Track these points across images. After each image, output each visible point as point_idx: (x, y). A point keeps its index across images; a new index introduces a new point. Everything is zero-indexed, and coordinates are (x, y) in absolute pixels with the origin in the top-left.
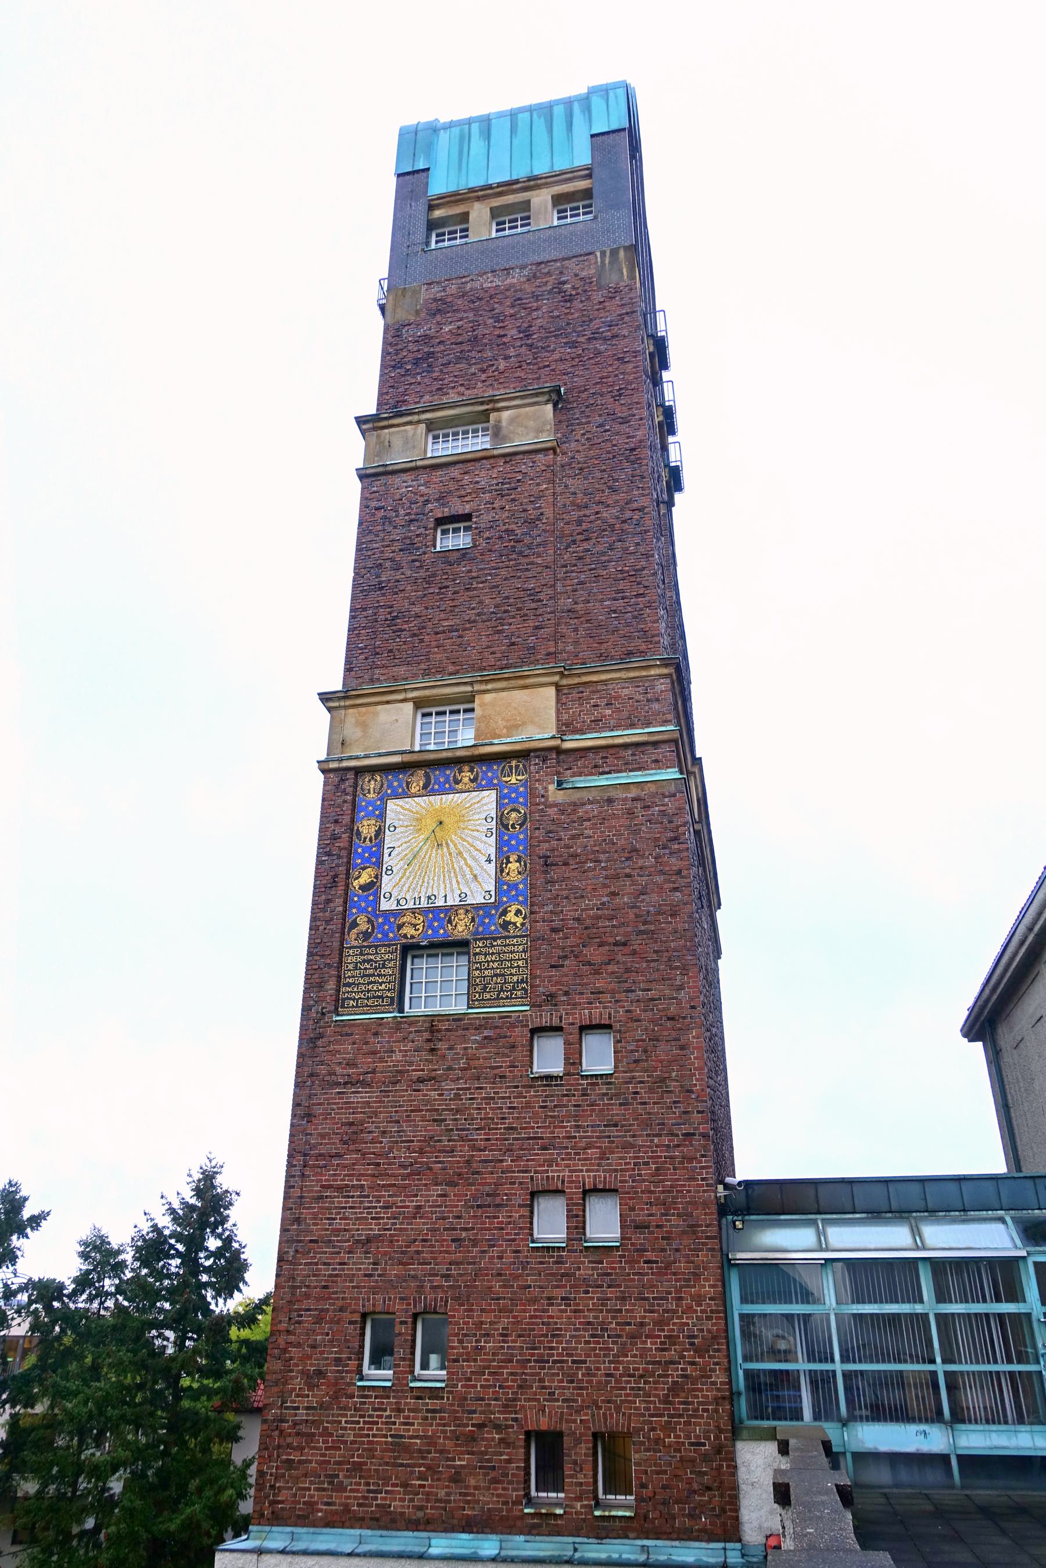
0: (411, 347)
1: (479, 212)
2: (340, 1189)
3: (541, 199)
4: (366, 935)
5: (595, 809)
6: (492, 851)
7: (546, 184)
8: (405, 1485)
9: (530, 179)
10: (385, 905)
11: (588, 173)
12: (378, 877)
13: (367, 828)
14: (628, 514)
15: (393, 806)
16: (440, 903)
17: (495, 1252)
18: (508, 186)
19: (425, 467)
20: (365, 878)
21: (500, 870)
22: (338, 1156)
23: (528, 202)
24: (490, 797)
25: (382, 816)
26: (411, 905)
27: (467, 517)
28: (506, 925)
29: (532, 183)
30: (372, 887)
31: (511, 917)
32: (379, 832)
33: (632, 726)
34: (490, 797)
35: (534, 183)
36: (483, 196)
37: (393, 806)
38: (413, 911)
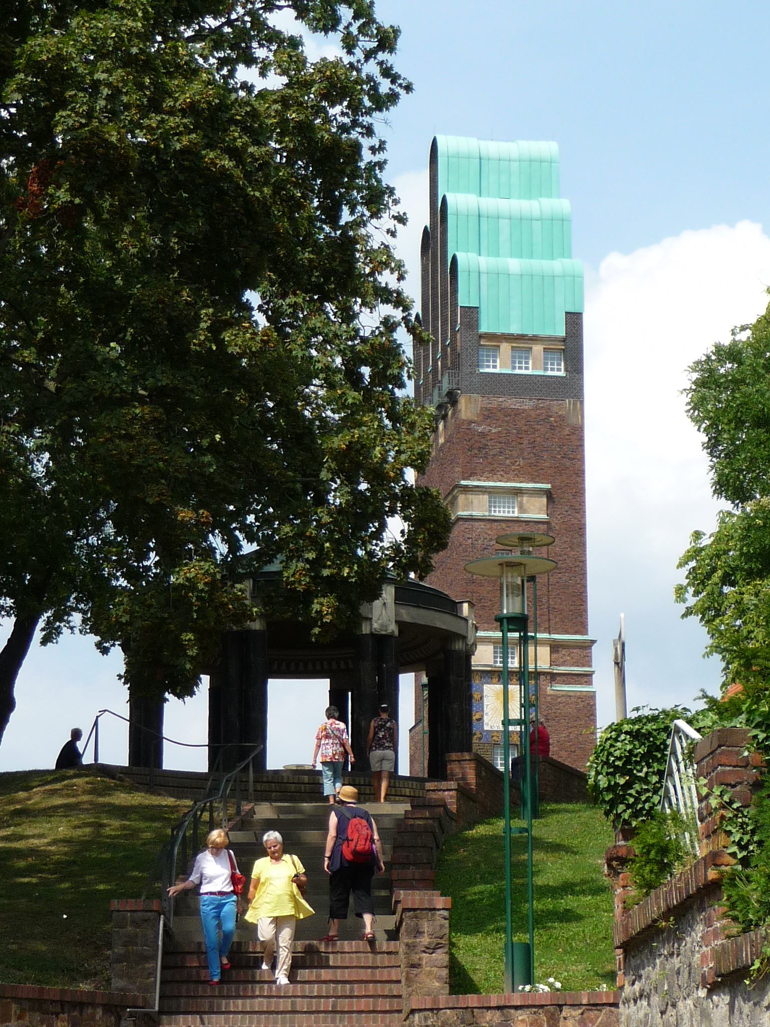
0: (477, 438)
1: (505, 347)
3: (538, 349)
4: (480, 739)
5: (564, 699)
9: (534, 336)
10: (486, 728)
11: (564, 340)
14: (578, 563)
15: (486, 687)
18: (521, 338)
19: (489, 520)
23: (531, 348)
30: (480, 719)
32: (482, 698)
33: (578, 666)
35: (535, 339)
37: (486, 687)
38: (497, 731)
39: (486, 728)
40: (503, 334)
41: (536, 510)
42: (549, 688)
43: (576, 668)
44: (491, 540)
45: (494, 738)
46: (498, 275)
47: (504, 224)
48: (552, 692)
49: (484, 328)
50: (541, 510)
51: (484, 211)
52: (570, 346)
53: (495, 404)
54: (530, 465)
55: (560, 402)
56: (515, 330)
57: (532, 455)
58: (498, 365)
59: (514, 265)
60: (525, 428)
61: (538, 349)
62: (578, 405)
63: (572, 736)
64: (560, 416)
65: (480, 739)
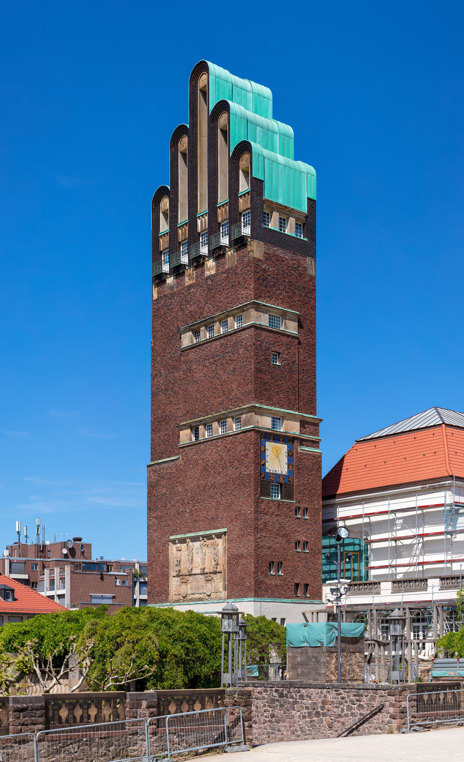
2: (265, 537)
4: (264, 478)
6: (287, 461)
8: (278, 591)
10: (267, 471)
12: (265, 462)
13: (262, 449)
16: (277, 473)
17: (290, 552)
20: (262, 463)
21: (288, 467)
22: (263, 530)
24: (286, 446)
25: (265, 446)
26: (272, 472)
27: (279, 353)
28: (289, 481)
30: (264, 465)
31: (290, 479)
32: (265, 450)
34: (286, 446)
38: (272, 474)
39: (267, 471)
41: (291, 328)
42: (299, 448)
43: (311, 437)
44: (270, 344)
45: (271, 478)
48: (300, 451)
50: (295, 329)
52: (308, 223)
54: (290, 297)
55: (304, 258)
57: (289, 291)
60: (286, 271)
61: (292, 221)
62: (313, 263)
63: (310, 481)
64: (304, 267)
65: (264, 478)
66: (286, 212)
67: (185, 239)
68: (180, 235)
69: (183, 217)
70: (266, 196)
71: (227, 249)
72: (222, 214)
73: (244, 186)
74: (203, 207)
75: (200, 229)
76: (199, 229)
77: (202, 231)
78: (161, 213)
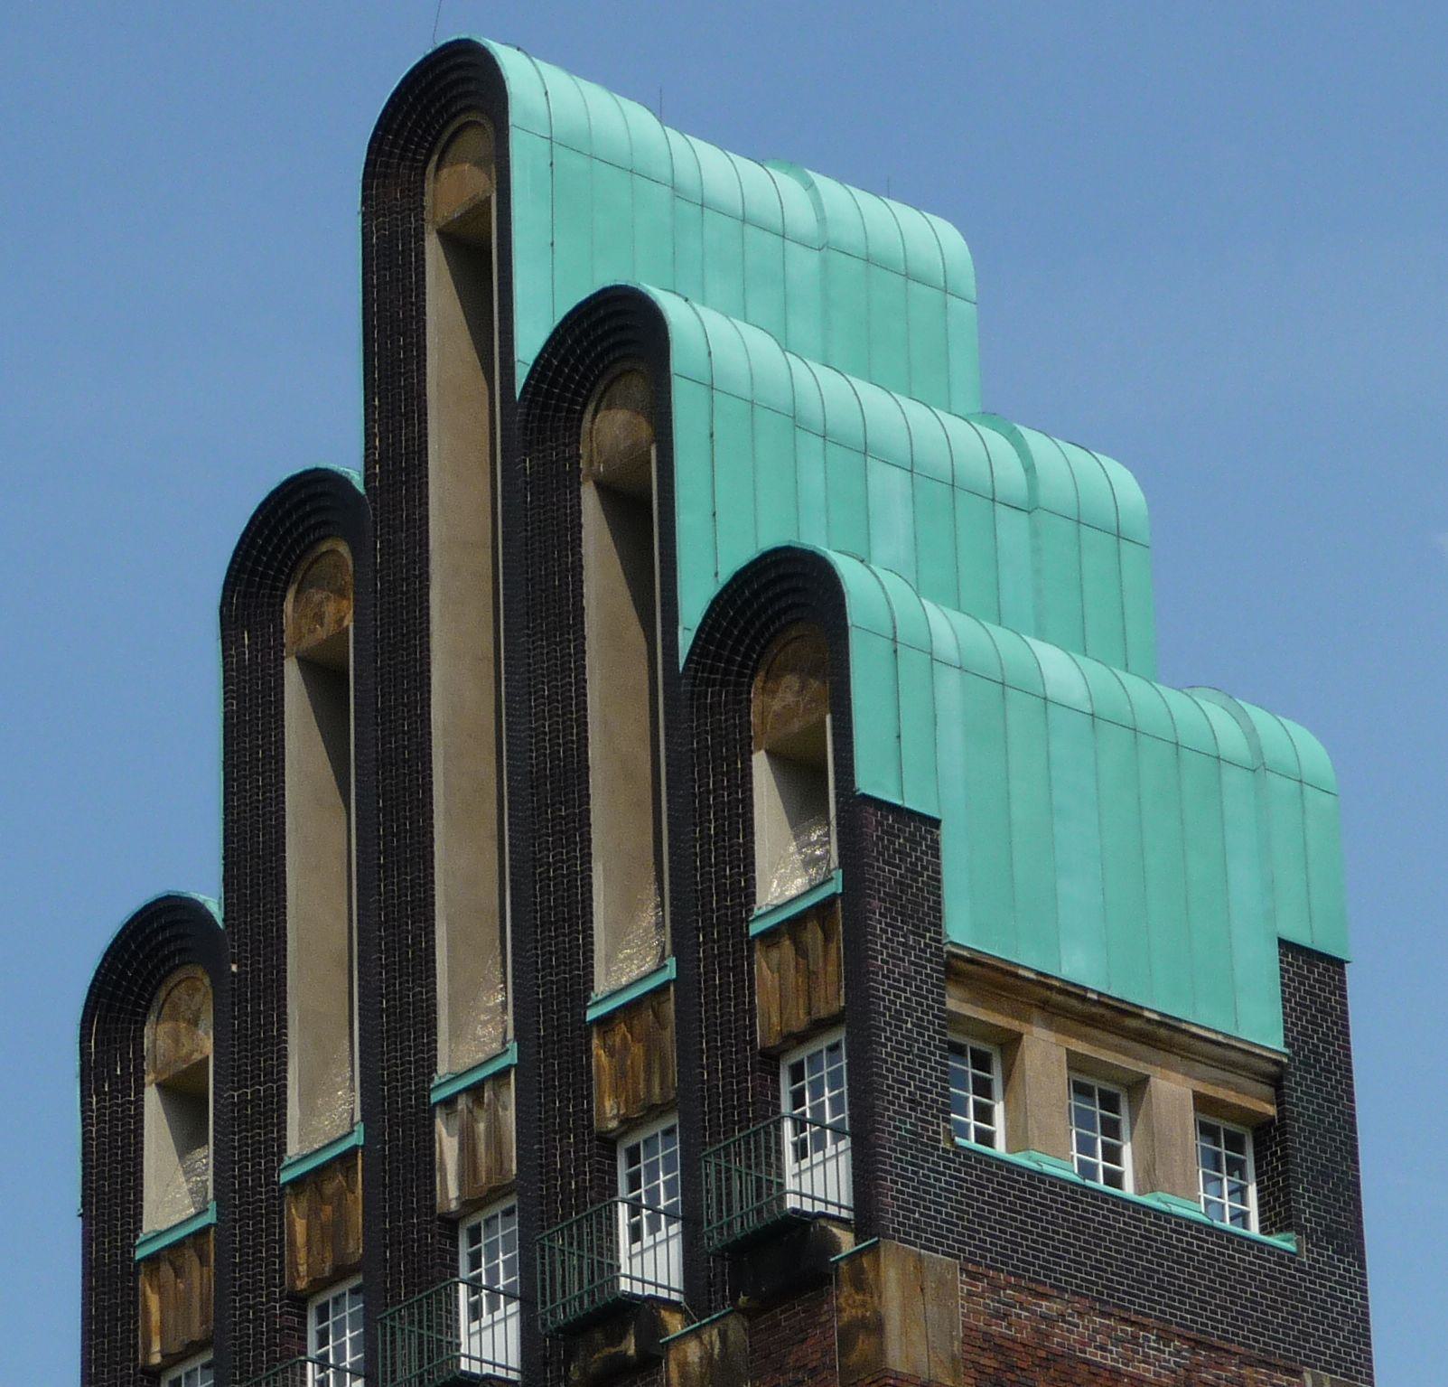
1: (1044, 1052)
7: (1186, 1049)
9: (1169, 1024)
11: (1276, 1078)
23: (1138, 1086)
29: (1163, 1032)
35: (1166, 1038)
36: (1057, 1006)
40: (1043, 980)
46: (1002, 685)
47: (888, 483)
49: (963, 926)
51: (810, 408)
52: (1292, 1122)
53: (1019, 1328)
56: (1079, 965)
58: (1029, 1127)
59: (1058, 668)
61: (1172, 1091)
66: (1117, 1040)
67: (341, 1273)
68: (300, 1239)
69: (322, 1112)
70: (963, 926)
71: (675, 1324)
72: (621, 1074)
73: (786, 870)
74: (474, 1030)
75: (453, 1192)
76: (450, 1191)
77: (472, 1204)
78: (152, 1097)
